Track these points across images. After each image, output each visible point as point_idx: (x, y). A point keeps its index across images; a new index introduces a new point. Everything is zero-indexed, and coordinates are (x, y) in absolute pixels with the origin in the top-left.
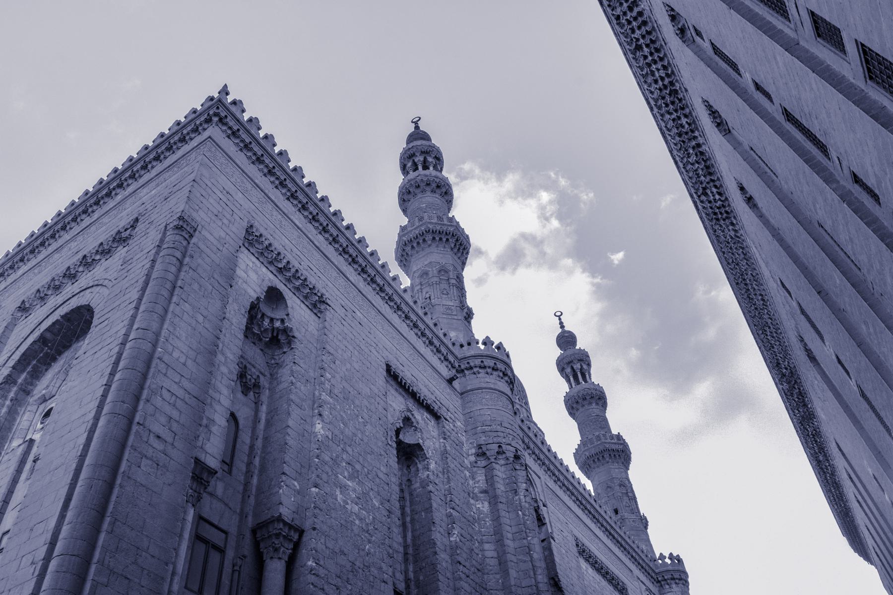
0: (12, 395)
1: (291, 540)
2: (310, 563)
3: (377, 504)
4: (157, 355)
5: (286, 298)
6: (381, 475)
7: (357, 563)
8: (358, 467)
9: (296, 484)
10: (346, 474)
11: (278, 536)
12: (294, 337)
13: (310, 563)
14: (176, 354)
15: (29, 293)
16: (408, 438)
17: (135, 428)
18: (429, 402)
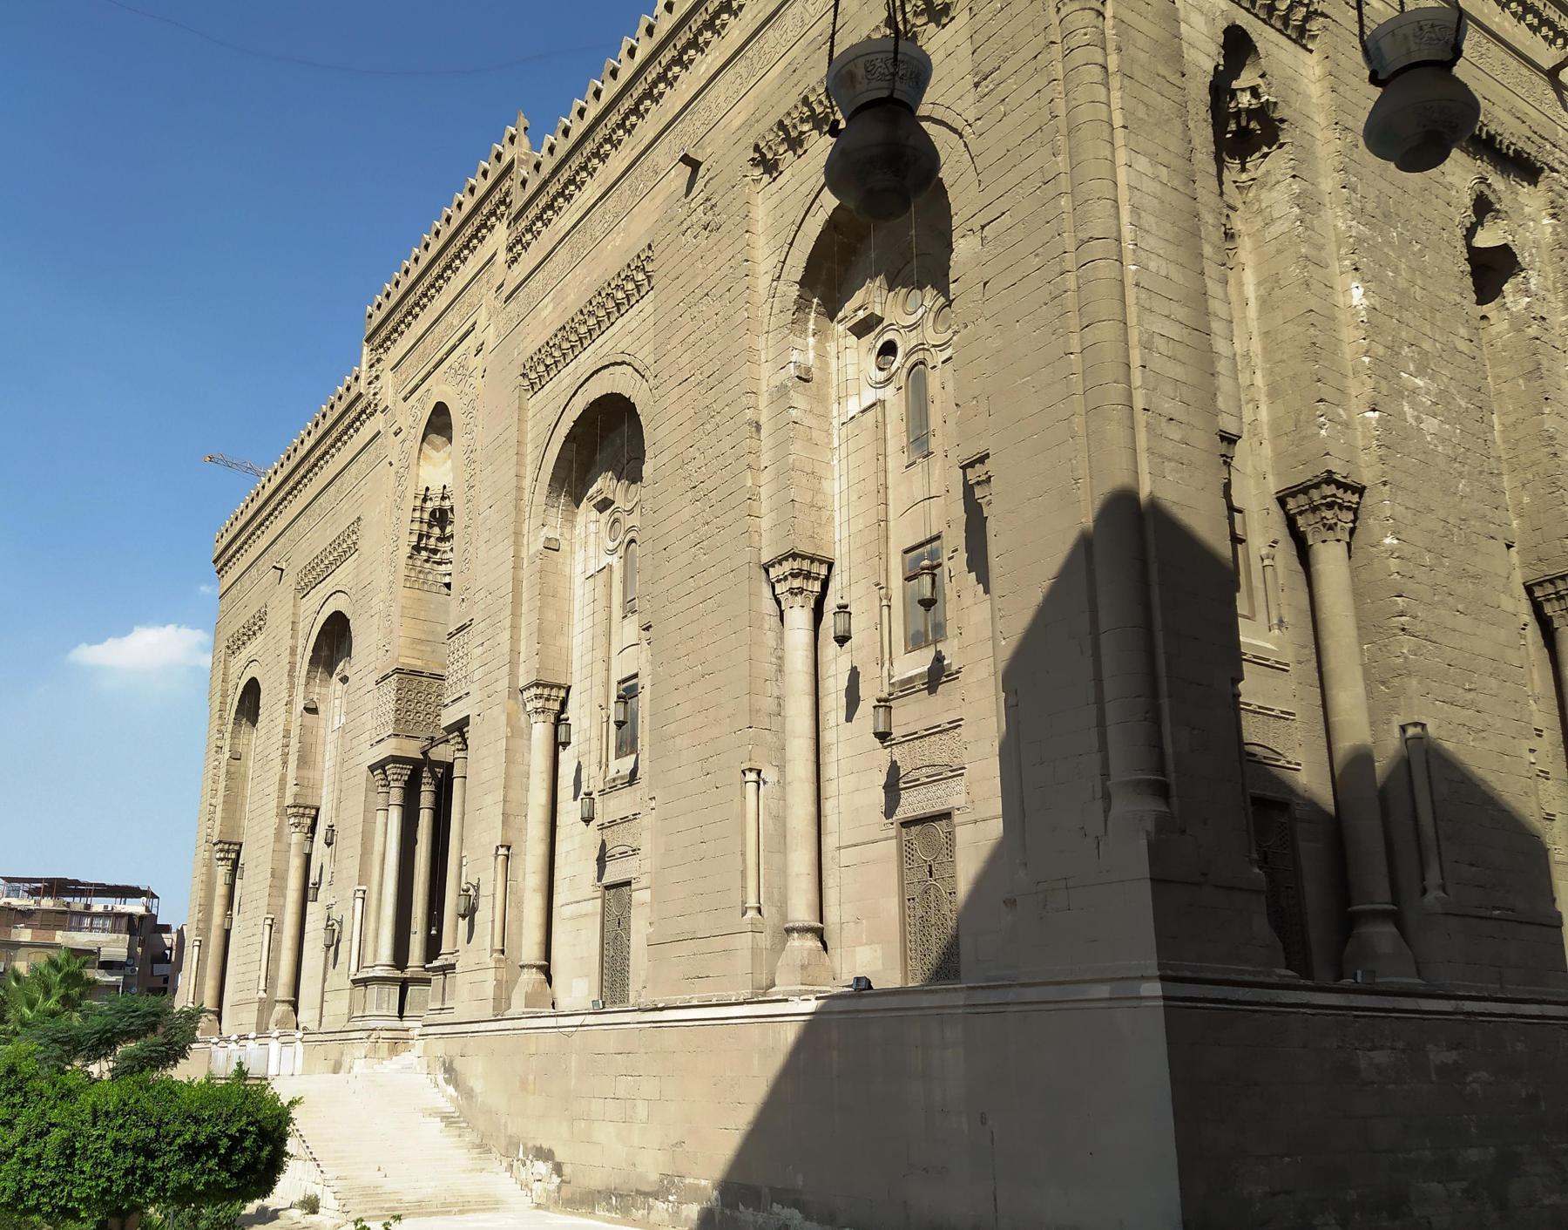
0: (811, 326)
1: (1349, 508)
2: (1388, 541)
3: (1463, 403)
4: (1129, 281)
5: (1254, 36)
6: (1463, 346)
7: (1450, 520)
8: (1426, 346)
9: (1341, 411)
10: (1412, 367)
11: (1330, 506)
12: (1282, 121)
13: (1388, 541)
14: (1153, 266)
15: (762, 127)
16: (1486, 238)
17: (1141, 418)
18: (1520, 145)
